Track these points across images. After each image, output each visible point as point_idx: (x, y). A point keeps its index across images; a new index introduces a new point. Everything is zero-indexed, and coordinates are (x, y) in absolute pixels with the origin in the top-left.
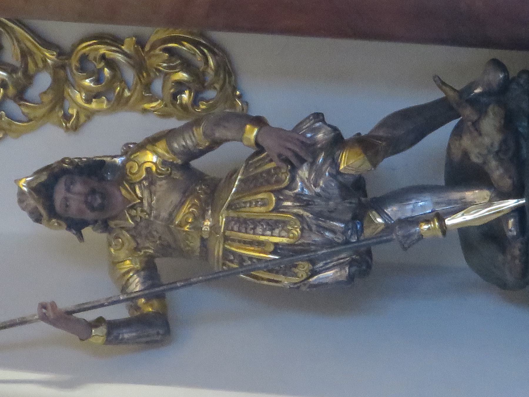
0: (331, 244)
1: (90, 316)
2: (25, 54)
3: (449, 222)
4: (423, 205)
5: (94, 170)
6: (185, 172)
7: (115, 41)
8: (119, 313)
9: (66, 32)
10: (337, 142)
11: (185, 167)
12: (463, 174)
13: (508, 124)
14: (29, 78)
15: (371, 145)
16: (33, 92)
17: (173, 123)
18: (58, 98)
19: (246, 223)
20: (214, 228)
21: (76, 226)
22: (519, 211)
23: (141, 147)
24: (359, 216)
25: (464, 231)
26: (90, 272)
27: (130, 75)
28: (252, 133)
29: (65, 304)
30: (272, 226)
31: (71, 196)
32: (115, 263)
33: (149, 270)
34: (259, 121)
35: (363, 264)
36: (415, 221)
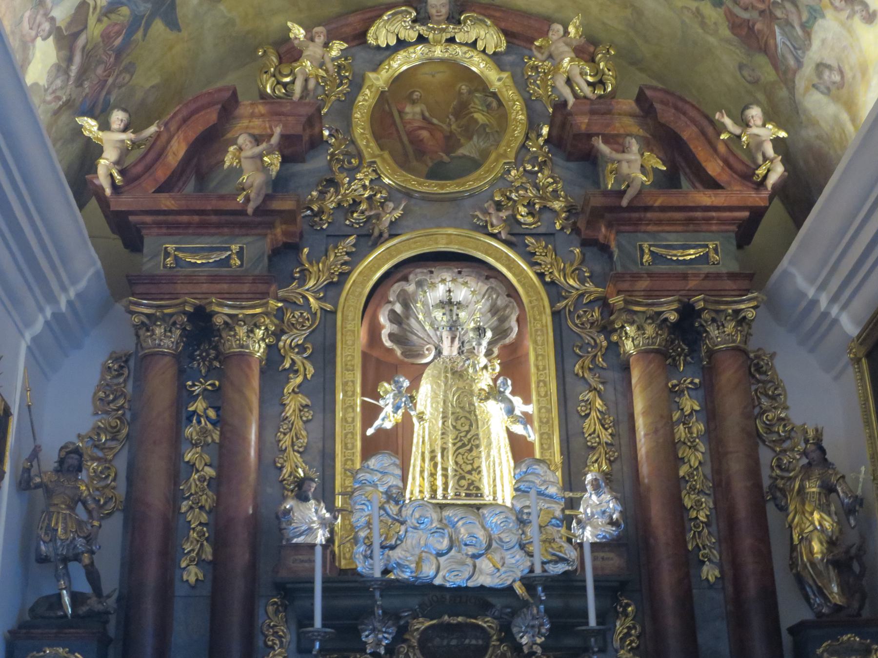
0: (57, 549)
1: (35, 463)
2: (111, 449)
3: (65, 592)
6: (77, 500)
7: (114, 480)
9: (121, 464)
11: (80, 500)
13: (99, 613)
14: (102, 449)
16: (96, 450)
18: (98, 459)
19: (65, 519)
20: (62, 509)
22: (66, 616)
25: (59, 596)
27: (102, 484)
29: (42, 455)
30: (65, 529)
31: (73, 460)
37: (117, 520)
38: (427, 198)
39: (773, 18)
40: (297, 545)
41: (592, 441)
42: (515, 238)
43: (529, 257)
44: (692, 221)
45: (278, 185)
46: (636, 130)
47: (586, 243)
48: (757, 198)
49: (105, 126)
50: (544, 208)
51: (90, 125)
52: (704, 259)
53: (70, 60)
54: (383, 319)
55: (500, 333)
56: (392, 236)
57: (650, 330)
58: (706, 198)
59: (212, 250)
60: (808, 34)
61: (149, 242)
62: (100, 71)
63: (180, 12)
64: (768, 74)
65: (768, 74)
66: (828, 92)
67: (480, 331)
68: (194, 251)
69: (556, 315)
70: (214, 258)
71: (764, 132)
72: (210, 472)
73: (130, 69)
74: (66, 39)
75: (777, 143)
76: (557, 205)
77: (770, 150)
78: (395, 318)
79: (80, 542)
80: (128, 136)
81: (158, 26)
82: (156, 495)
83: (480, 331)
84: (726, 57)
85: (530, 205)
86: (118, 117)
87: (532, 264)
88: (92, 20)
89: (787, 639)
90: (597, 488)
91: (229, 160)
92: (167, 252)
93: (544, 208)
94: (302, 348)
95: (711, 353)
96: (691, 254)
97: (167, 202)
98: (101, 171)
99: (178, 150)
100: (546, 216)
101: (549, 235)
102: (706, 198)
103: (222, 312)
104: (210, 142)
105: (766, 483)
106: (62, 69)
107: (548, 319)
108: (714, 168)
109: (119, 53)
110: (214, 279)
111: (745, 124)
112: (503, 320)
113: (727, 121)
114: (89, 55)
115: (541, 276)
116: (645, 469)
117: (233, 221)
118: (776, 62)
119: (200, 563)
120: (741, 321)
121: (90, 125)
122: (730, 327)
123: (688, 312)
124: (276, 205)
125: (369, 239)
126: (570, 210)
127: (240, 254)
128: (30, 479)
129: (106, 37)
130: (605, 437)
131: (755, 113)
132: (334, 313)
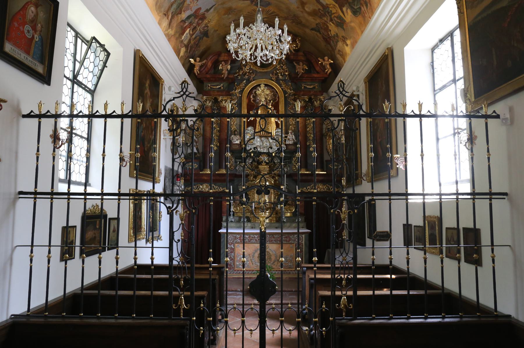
37: (202, 137)
38: (260, 72)
39: (330, 39)
40: (234, 144)
41: (291, 123)
42: (277, 81)
43: (280, 85)
44: (313, 80)
45: (229, 72)
46: (303, 58)
47: (291, 82)
48: (326, 76)
49: (195, 61)
50: (284, 74)
51: (192, 60)
52: (314, 88)
53: (188, 49)
54: (251, 97)
55: (274, 100)
56: (254, 80)
57: (302, 102)
58: (316, 76)
59: (218, 85)
60: (337, 44)
61: (205, 83)
62: (194, 49)
63: (209, 35)
64: (330, 49)
65: (330, 49)
66: (340, 55)
67: (270, 101)
68: (214, 86)
69: (285, 98)
70: (218, 87)
71: (327, 62)
72: (218, 129)
73: (199, 47)
74: (187, 46)
75: (331, 64)
76: (287, 73)
77: (328, 66)
78: (253, 97)
80: (200, 64)
81: (205, 38)
82: (208, 135)
83: (270, 101)
84: (323, 44)
85: (281, 74)
86: (198, 59)
87: (281, 86)
88: (192, 41)
89: (325, 163)
90: (291, 133)
91: (220, 68)
92: (209, 86)
93: (284, 74)
94: (235, 104)
95: (315, 107)
96: (312, 87)
97: (208, 76)
98: (195, 71)
99: (210, 64)
100: (285, 76)
101: (284, 80)
102: (316, 76)
103: (220, 98)
104: (216, 64)
105: (324, 132)
106: (186, 52)
107: (283, 98)
108: (318, 69)
109: (197, 45)
110: (218, 91)
111: (324, 60)
112: (276, 97)
113: (320, 60)
114: (191, 47)
115: (282, 89)
116: (300, 129)
117: (222, 80)
118: (331, 46)
119: (217, 146)
120: (320, 100)
121: (192, 60)
122: (318, 102)
123: (310, 99)
124: (230, 76)
125: (249, 81)
126: (289, 75)
127: (223, 86)
129: (194, 43)
130: (294, 123)
131: (326, 58)
132: (241, 96)
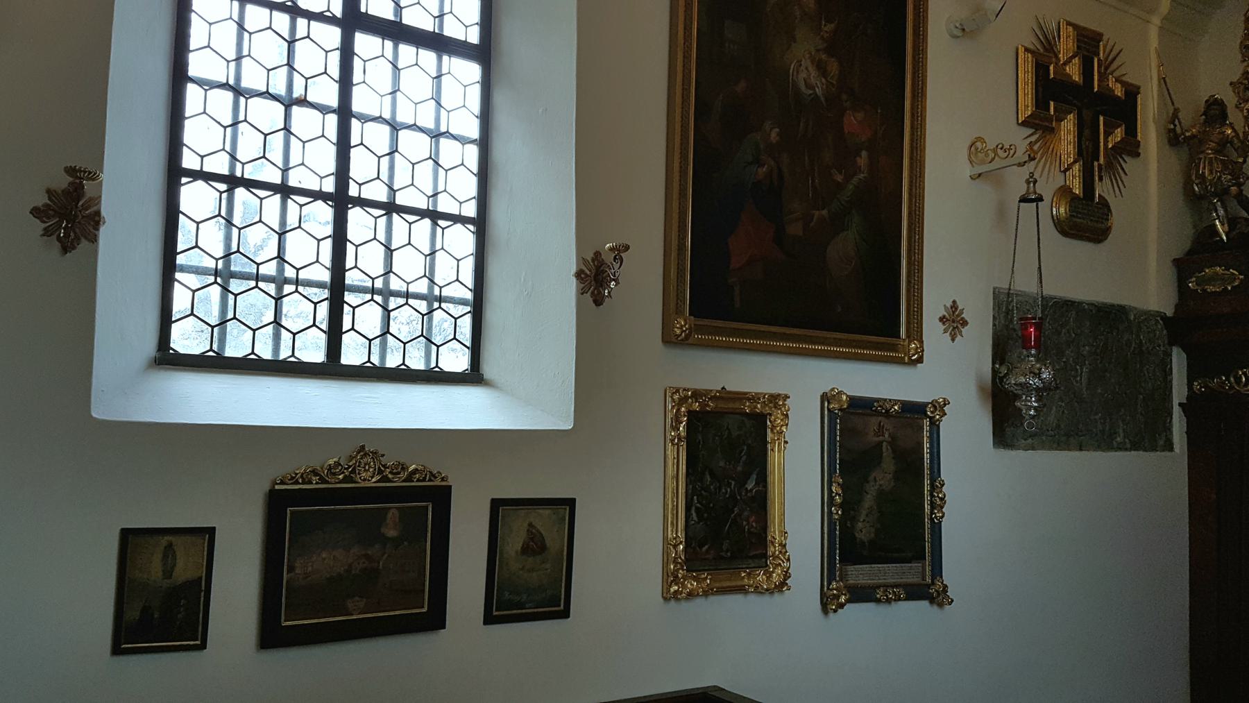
4: (1221, 212)
5: (1224, 116)
8: (1178, 130)
10: (1239, 185)
12: (1232, 222)
15: (1240, 195)
17: (1241, 135)
19: (1211, 163)
21: (1205, 114)
23: (1233, 128)
24: (1215, 195)
25: (1215, 225)
26: (1189, 119)
28: (1241, 160)
29: (1180, 115)
32: (1193, 127)
33: (1193, 136)
34: (1245, 161)
35: (1200, 197)
36: (1216, 211)
79: (1226, 178)
128: (1176, 136)
